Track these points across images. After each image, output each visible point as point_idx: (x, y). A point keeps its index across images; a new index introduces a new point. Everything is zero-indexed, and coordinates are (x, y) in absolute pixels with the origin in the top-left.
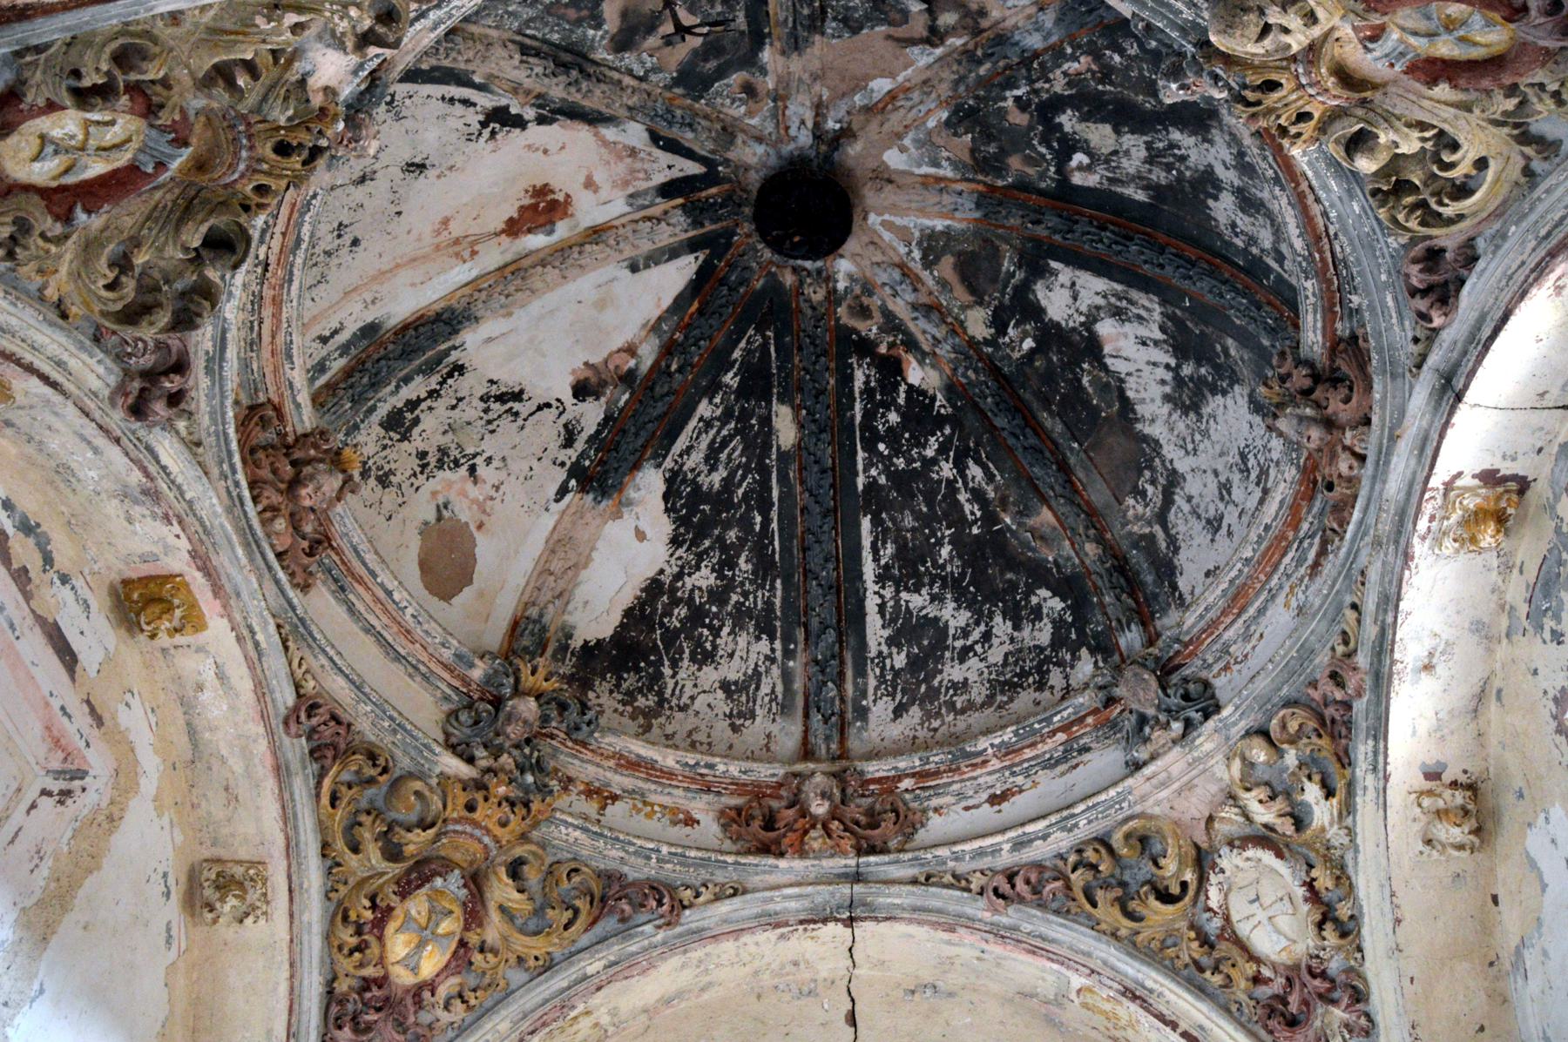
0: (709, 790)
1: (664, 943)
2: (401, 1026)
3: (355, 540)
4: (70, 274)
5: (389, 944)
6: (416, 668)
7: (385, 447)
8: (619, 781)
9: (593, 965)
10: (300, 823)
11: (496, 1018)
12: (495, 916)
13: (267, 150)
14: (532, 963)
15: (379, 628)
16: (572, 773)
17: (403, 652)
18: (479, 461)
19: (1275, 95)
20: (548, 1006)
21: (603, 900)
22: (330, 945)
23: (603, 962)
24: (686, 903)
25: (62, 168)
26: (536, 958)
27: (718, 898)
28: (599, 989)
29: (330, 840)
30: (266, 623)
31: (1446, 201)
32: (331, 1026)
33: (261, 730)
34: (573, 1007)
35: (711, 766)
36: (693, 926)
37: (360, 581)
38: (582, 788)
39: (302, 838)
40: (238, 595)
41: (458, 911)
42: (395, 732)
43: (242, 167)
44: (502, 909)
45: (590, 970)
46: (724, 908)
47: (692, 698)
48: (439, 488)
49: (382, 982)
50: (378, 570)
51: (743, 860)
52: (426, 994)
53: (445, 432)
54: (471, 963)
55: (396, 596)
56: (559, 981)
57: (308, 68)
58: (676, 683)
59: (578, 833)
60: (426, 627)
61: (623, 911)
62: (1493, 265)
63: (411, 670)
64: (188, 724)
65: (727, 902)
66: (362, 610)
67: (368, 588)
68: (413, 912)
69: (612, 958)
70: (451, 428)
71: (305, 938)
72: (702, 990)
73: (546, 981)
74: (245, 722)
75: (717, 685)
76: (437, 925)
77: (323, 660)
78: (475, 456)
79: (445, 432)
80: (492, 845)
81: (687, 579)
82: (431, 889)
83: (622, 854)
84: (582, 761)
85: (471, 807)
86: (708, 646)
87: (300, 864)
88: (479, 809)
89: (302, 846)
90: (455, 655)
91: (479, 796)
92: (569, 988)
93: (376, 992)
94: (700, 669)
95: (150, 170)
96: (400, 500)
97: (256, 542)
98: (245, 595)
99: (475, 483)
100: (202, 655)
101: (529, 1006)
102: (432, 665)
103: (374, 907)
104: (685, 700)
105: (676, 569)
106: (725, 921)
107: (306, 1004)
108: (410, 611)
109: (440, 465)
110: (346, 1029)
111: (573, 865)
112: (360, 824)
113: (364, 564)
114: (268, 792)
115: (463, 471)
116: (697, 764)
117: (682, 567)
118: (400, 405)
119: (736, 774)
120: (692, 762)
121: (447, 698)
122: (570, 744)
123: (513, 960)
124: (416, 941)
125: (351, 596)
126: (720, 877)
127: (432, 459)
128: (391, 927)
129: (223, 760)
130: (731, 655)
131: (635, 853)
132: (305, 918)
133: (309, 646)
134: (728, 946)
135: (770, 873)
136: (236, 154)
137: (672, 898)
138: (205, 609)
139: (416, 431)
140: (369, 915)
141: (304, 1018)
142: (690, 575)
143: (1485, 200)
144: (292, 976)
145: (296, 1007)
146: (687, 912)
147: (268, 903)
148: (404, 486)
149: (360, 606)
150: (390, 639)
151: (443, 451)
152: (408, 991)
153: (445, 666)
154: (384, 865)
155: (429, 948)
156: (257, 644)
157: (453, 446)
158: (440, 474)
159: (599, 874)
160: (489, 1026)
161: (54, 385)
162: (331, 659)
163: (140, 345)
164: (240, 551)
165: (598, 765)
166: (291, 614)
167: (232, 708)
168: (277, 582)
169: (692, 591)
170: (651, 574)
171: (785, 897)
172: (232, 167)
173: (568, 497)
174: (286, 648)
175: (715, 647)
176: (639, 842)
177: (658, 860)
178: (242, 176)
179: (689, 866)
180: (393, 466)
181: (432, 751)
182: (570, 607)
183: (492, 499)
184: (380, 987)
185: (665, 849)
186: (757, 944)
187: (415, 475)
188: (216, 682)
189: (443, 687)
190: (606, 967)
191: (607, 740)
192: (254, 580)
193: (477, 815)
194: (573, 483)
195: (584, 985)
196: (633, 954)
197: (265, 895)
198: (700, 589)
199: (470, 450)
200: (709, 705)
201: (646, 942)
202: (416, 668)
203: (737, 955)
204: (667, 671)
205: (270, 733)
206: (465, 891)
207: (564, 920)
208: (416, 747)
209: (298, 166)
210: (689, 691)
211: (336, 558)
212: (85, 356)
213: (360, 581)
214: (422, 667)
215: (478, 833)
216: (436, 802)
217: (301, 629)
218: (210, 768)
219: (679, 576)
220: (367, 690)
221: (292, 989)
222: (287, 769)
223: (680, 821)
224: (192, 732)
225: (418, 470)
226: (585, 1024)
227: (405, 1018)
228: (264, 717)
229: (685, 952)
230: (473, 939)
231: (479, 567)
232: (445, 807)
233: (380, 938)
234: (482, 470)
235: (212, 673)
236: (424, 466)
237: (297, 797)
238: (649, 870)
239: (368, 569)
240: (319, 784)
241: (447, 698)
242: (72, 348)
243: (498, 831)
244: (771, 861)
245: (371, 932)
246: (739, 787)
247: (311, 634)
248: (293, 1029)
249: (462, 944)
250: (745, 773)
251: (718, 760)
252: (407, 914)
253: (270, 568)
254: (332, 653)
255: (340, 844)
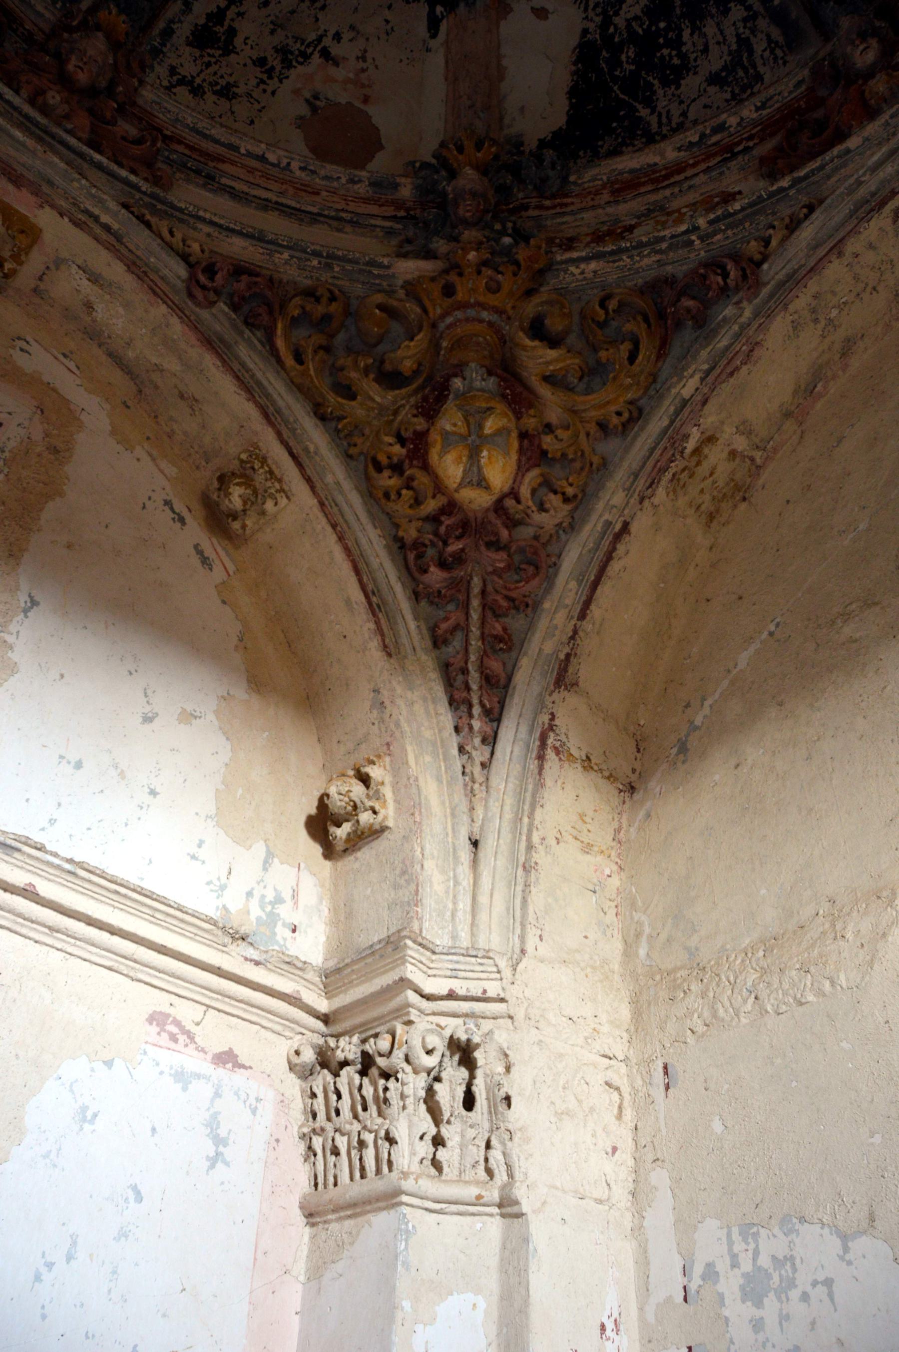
0: (734, 155)
1: (756, 315)
2: (495, 545)
3: (189, 120)
5: (440, 472)
6: (339, 219)
7: (208, 65)
8: (626, 209)
9: (689, 387)
10: (270, 390)
11: (605, 495)
12: (545, 391)
14: (615, 420)
15: (274, 198)
16: (570, 233)
17: (315, 210)
18: (327, 42)
20: (658, 452)
21: (662, 316)
22: (377, 501)
23: (697, 377)
24: (758, 257)
26: (619, 414)
27: (793, 225)
28: (705, 402)
29: (320, 400)
30: (101, 201)
32: (417, 575)
33: (164, 308)
34: (686, 437)
35: (721, 128)
36: (781, 276)
37: (220, 159)
38: (588, 239)
39: (281, 403)
40: (50, 183)
41: (500, 407)
42: (329, 266)
44: (547, 379)
45: (686, 392)
46: (807, 233)
47: (684, 114)
48: (299, 85)
49: (451, 507)
50: (234, 140)
51: (802, 173)
52: (509, 503)
53: (272, 32)
54: (544, 453)
55: (272, 158)
56: (657, 424)
58: (660, 115)
59: (593, 265)
60: (322, 173)
61: (688, 311)
63: (335, 224)
64: (110, 355)
65: (807, 223)
66: (245, 188)
67: (233, 163)
68: (448, 427)
69: (705, 367)
70: (276, 26)
71: (340, 499)
72: (845, 353)
73: (642, 429)
74: (146, 311)
75: (704, 85)
76: (481, 427)
77: (207, 229)
78: (320, 39)
79: (272, 32)
80: (494, 318)
81: (616, 20)
82: (457, 397)
83: (658, 257)
84: (572, 213)
85: (449, 291)
86: (676, 61)
87: (293, 431)
88: (459, 288)
89: (286, 412)
90: (370, 184)
91: (453, 277)
92: (672, 422)
93: (447, 521)
94: (678, 87)
96: (257, 106)
97: (46, 132)
98: (58, 180)
99: (336, 64)
100: (63, 267)
101: (635, 466)
102: (352, 207)
103: (402, 441)
104: (675, 120)
105: (598, 19)
106: (816, 247)
107: (375, 563)
108: (295, 165)
109: (288, 64)
110: (432, 569)
111: (602, 293)
112: (342, 369)
113: (217, 142)
114: (213, 370)
115: (316, 59)
116: (703, 136)
117: (604, 13)
118: (202, 21)
119: (755, 115)
120: (695, 138)
121: (390, 233)
122: (547, 203)
123: (593, 428)
124: (466, 452)
125: (224, 181)
126: (785, 211)
127: (275, 62)
128: (434, 456)
129: (158, 368)
130: (706, 50)
131: (670, 248)
132: (329, 479)
133: (181, 221)
134: (835, 269)
135: (845, 165)
137: (734, 261)
138: (23, 210)
139: (238, 41)
140: (398, 450)
141: (380, 576)
142: (617, 14)
144: (341, 538)
145: (362, 566)
146: (765, 266)
147: (280, 481)
148: (254, 94)
149: (239, 186)
150: (293, 204)
151: (283, 51)
152: (488, 510)
153: (366, 200)
154: (390, 396)
155: (485, 453)
156: (107, 228)
157: (290, 41)
158: (293, 73)
159: (642, 291)
160: (600, 505)
162: (212, 223)
164: (18, 134)
165: (594, 207)
166: (138, 196)
167: (127, 305)
168: (99, 167)
169: (629, 26)
170: (574, 41)
171: (874, 169)
173: (443, 27)
174: (148, 225)
175: (683, 57)
176: (667, 233)
177: (701, 238)
179: (741, 222)
180: (232, 80)
181: (381, 266)
182: (507, 121)
183: (363, 70)
184: (450, 515)
185: (702, 222)
186: (871, 246)
187: (262, 81)
188: (95, 288)
189: (379, 222)
190: (702, 380)
191: (587, 176)
192: (56, 160)
193: (460, 296)
194: (439, 9)
195: (687, 410)
196: (727, 348)
197: (271, 472)
198: (636, 18)
199: (312, 36)
200: (705, 106)
201: (736, 327)
202: (339, 219)
203: (856, 278)
204: (643, 112)
205: (176, 308)
206: (492, 380)
207: (625, 354)
208: (361, 271)
210: (676, 112)
211: (181, 149)
213: (220, 159)
214: (344, 215)
215: (471, 312)
216: (412, 309)
217: (159, 206)
218: (156, 387)
219: (607, 22)
220: (270, 237)
221: (347, 551)
222: (222, 341)
223: (718, 203)
224: (116, 359)
225: (265, 77)
226: (715, 455)
227: (496, 534)
228: (164, 298)
229: (786, 307)
230: (530, 423)
231: (382, 132)
232: (425, 310)
233: (426, 467)
234: (336, 50)
235: (85, 282)
236: (270, 72)
237: (251, 366)
238: (699, 252)
239: (223, 145)
240: (274, 352)
241: (390, 233)
243: (493, 300)
244: (835, 151)
245: (411, 466)
246: (767, 128)
247: (173, 207)
248: (370, 587)
249: (523, 435)
250: (763, 106)
251: (724, 116)
252: (445, 435)
253: (81, 155)
254: (208, 216)
255: (332, 399)
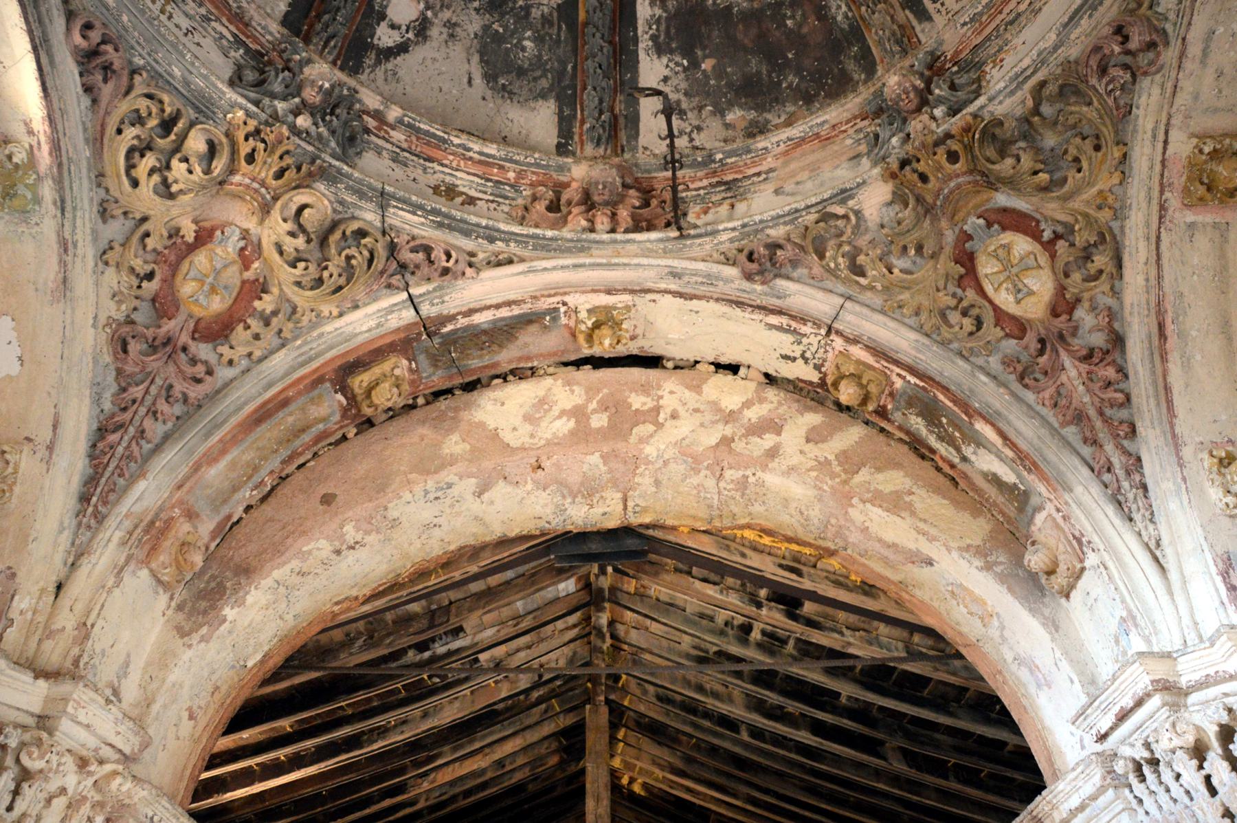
4: (1093, 186)
13: (933, 184)
19: (275, 169)
25: (1029, 273)
31: (135, 142)
43: (952, 184)
57: (884, 209)
62: (78, 112)
95: (996, 226)
136: (951, 192)
143: (115, 156)
161: (1167, 133)
163: (1111, 87)
172: (959, 187)
178: (958, 176)
209: (922, 163)
212: (1140, 121)
242: (1139, 138)
